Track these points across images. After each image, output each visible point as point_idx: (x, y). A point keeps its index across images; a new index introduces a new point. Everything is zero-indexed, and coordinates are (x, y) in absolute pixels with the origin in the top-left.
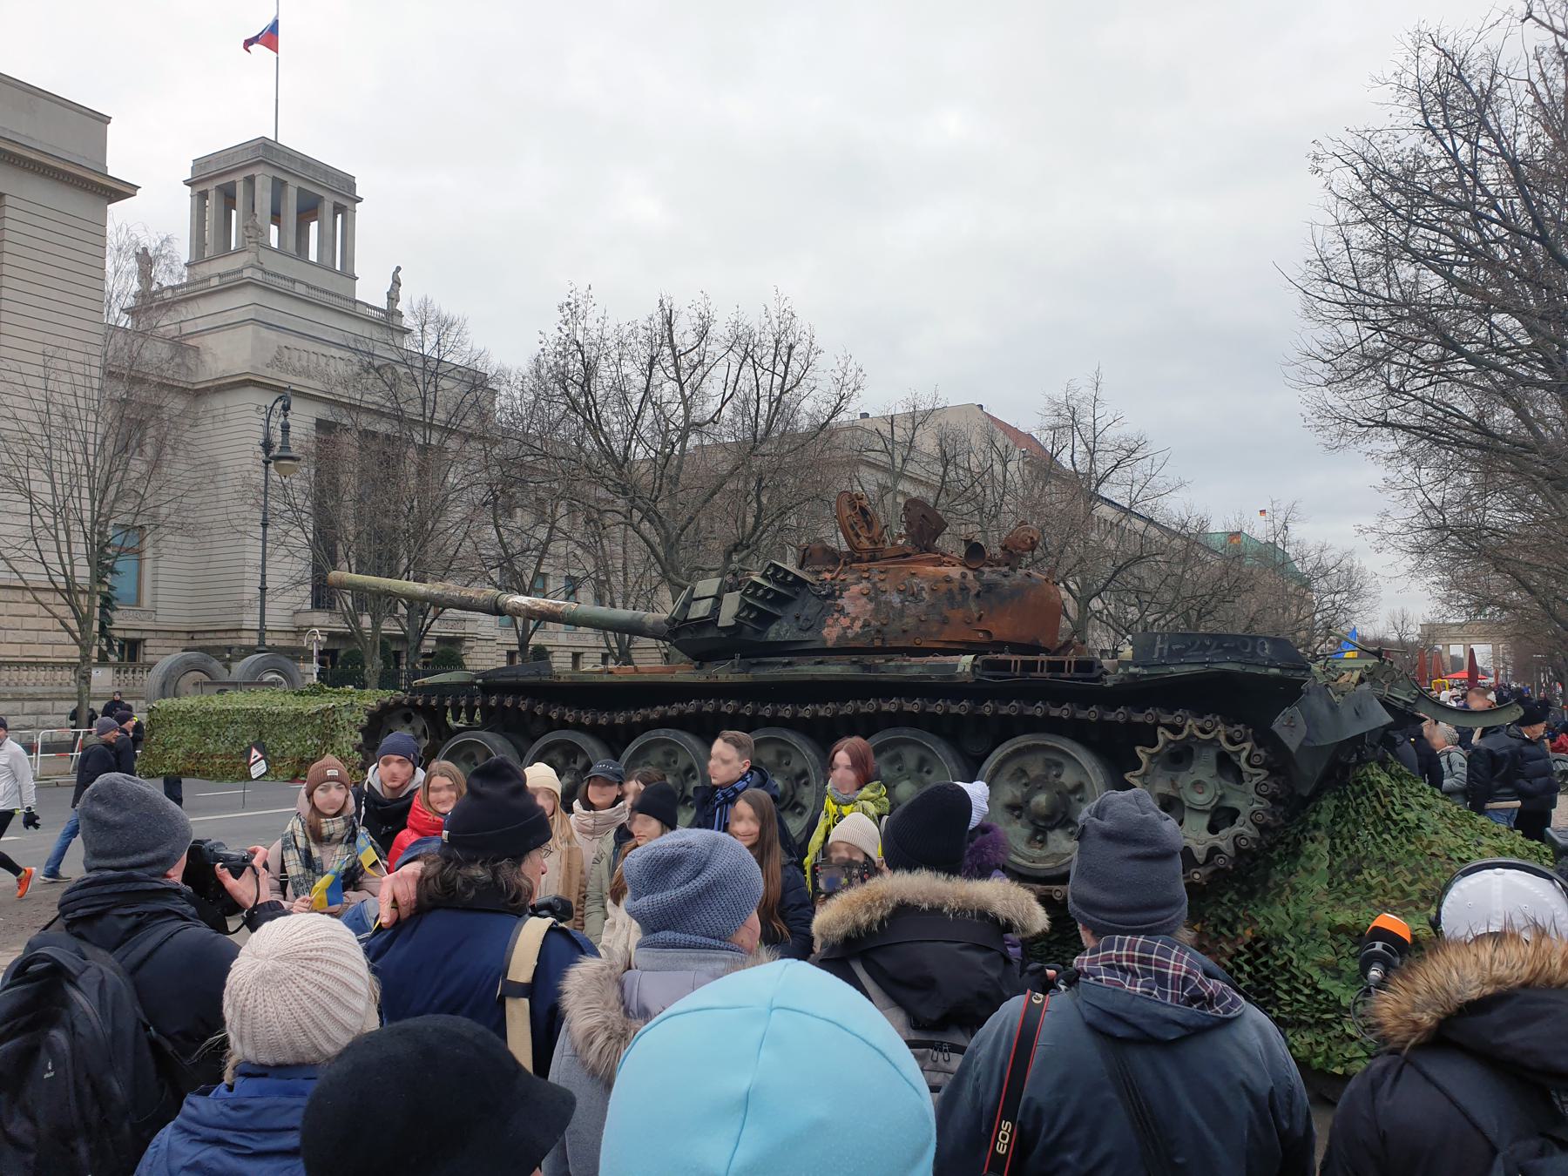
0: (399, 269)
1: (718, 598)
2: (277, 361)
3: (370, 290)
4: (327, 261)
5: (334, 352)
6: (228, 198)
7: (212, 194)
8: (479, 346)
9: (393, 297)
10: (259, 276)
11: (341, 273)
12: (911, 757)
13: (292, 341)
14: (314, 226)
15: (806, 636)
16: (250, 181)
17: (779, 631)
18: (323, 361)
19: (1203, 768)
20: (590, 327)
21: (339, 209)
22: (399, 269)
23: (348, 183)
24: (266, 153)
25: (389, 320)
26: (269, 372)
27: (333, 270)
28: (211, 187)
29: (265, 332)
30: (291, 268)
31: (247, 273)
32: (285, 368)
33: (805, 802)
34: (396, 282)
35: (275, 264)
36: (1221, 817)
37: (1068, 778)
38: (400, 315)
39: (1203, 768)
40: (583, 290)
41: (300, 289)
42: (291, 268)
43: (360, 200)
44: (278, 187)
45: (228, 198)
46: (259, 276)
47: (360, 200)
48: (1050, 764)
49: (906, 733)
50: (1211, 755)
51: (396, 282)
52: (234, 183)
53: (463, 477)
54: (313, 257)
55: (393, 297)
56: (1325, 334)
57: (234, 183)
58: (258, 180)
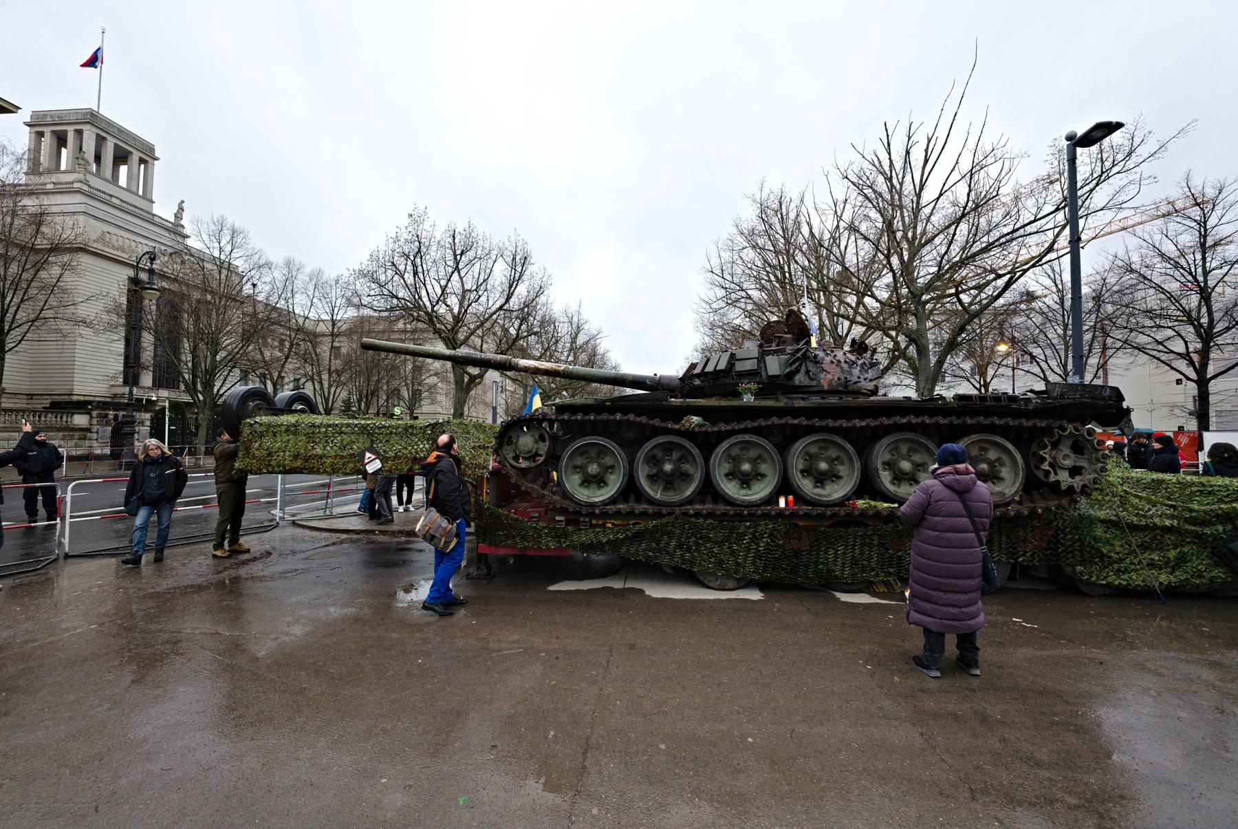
0: (183, 202)
1: (761, 359)
2: (101, 238)
3: (163, 209)
4: (134, 189)
5: (141, 240)
6: (61, 140)
7: (48, 135)
8: (258, 247)
9: (178, 216)
10: (86, 188)
11: (144, 197)
12: (904, 449)
13: (112, 230)
14: (123, 169)
15: (814, 383)
16: (79, 133)
17: (800, 379)
18: (134, 244)
19: (1065, 449)
20: (426, 230)
21: (142, 161)
22: (183, 202)
23: (152, 150)
24: (92, 118)
25: (176, 230)
26: (95, 245)
27: (137, 194)
28: (47, 130)
29: (92, 221)
30: (109, 188)
31: (76, 185)
32: (107, 244)
33: (841, 474)
34: (181, 209)
35: (96, 182)
36: (1075, 471)
37: (993, 455)
38: (183, 227)
39: (1065, 449)
40: (422, 208)
41: (114, 200)
42: (109, 188)
43: (157, 159)
44: (100, 141)
45: (61, 140)
46: (86, 188)
47: (157, 159)
48: (982, 449)
49: (908, 435)
50: (1069, 442)
51: (181, 209)
52: (66, 132)
53: (236, 316)
54: (123, 181)
55: (178, 216)
56: (711, 295)
57: (66, 132)
58: (85, 134)
